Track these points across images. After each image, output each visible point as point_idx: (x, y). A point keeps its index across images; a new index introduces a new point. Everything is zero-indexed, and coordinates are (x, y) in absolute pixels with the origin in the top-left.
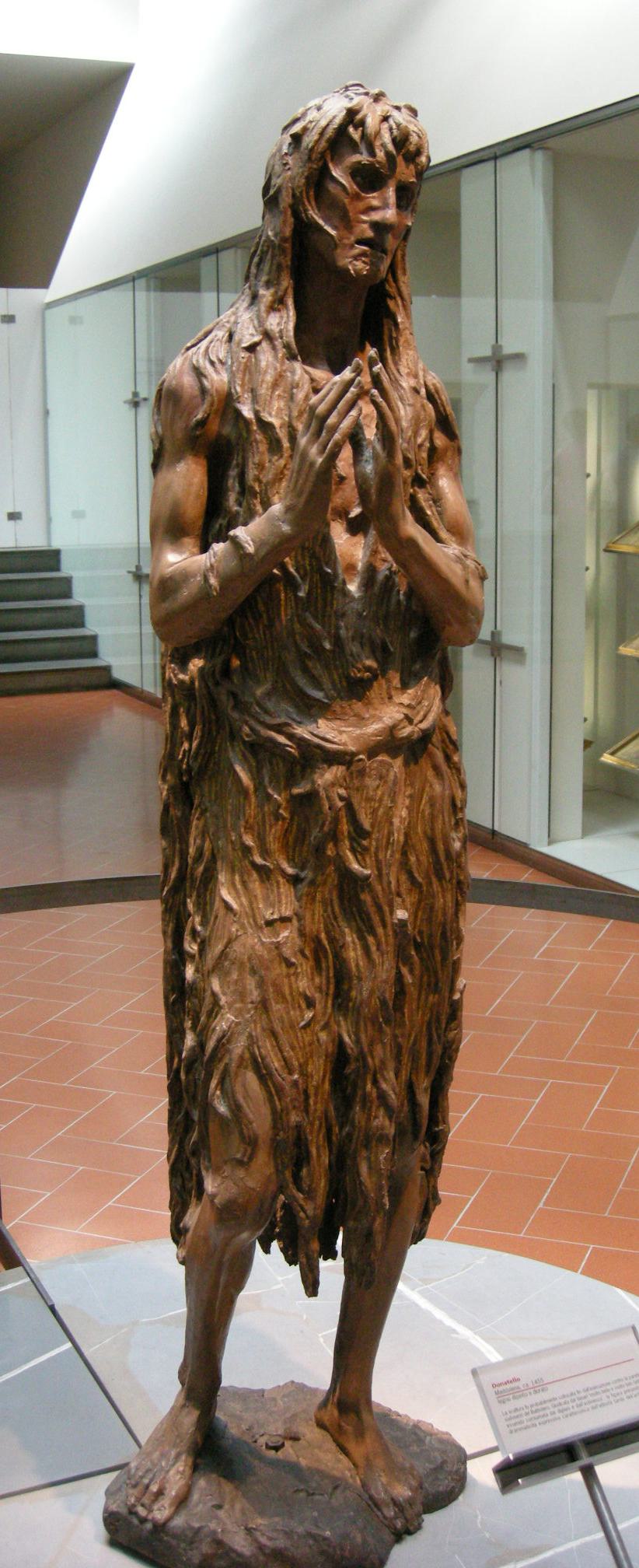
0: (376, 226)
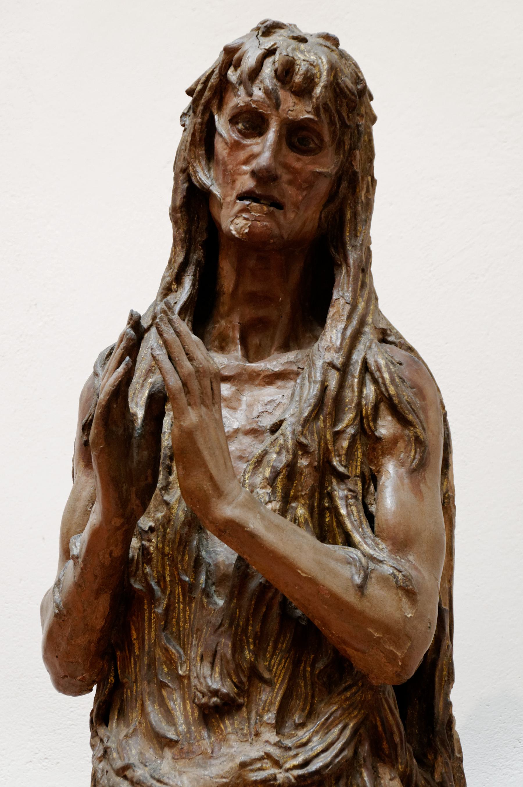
0: (253, 174)
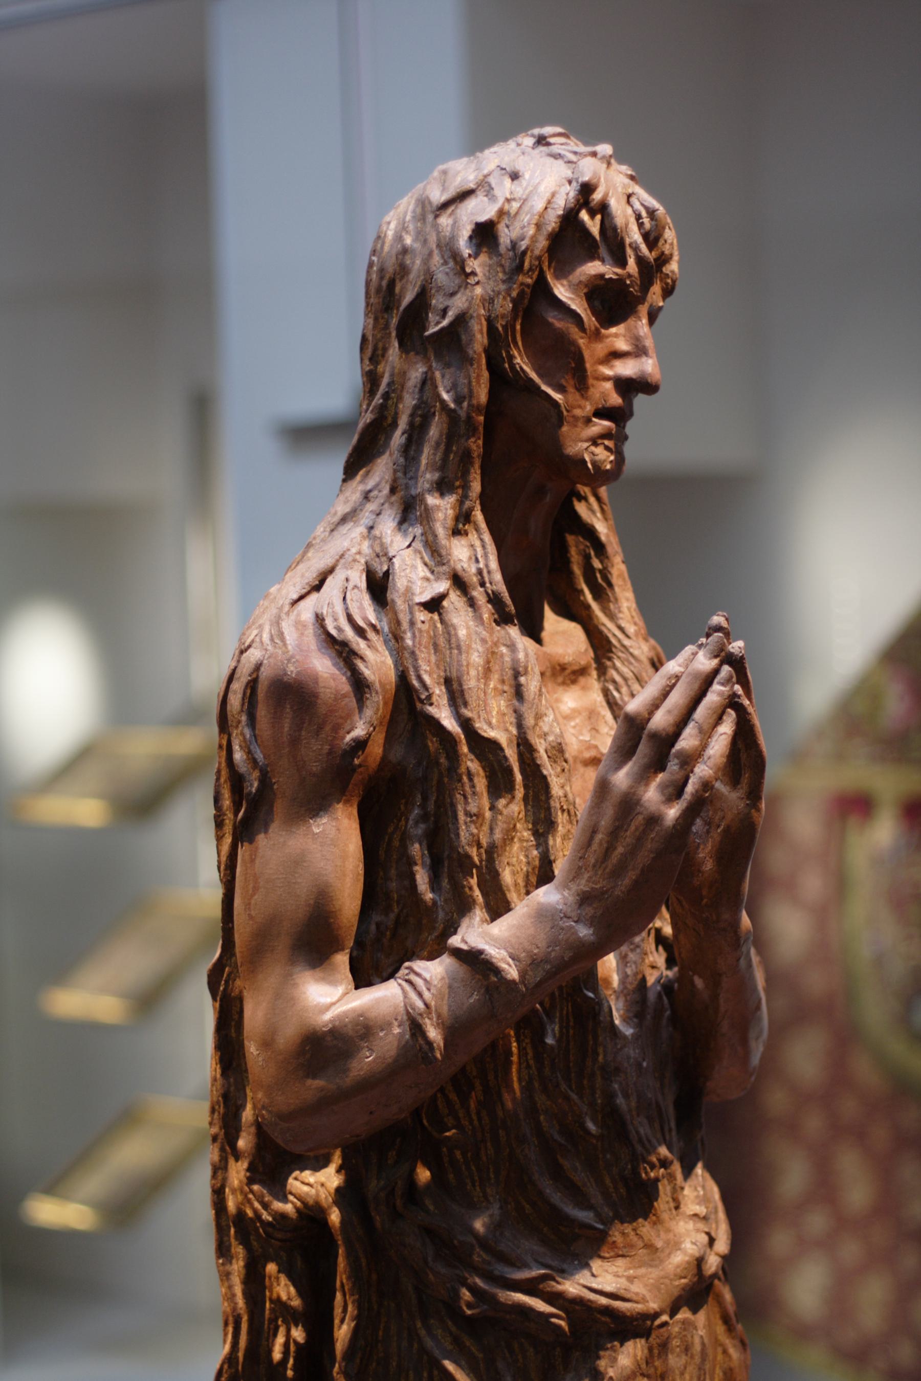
0: (627, 386)
